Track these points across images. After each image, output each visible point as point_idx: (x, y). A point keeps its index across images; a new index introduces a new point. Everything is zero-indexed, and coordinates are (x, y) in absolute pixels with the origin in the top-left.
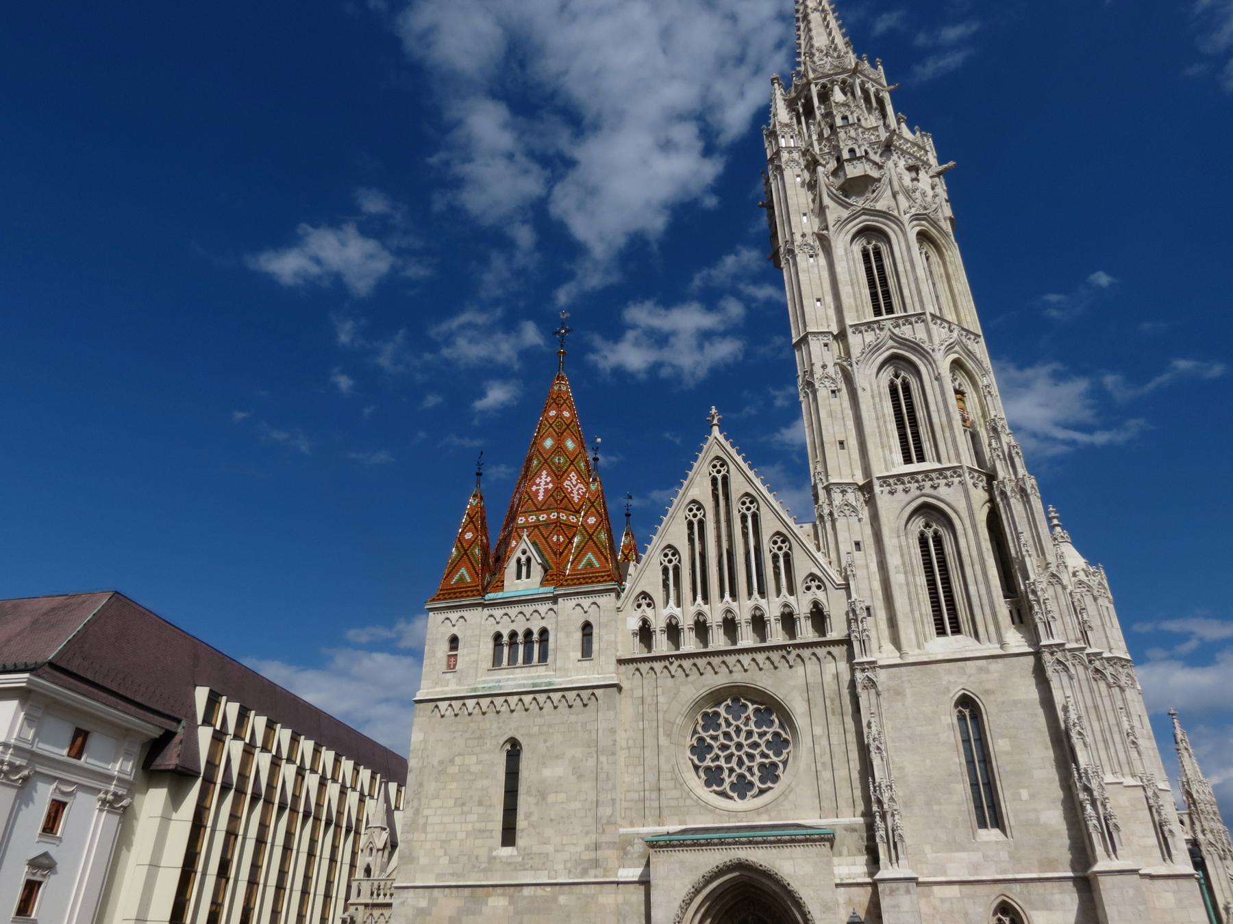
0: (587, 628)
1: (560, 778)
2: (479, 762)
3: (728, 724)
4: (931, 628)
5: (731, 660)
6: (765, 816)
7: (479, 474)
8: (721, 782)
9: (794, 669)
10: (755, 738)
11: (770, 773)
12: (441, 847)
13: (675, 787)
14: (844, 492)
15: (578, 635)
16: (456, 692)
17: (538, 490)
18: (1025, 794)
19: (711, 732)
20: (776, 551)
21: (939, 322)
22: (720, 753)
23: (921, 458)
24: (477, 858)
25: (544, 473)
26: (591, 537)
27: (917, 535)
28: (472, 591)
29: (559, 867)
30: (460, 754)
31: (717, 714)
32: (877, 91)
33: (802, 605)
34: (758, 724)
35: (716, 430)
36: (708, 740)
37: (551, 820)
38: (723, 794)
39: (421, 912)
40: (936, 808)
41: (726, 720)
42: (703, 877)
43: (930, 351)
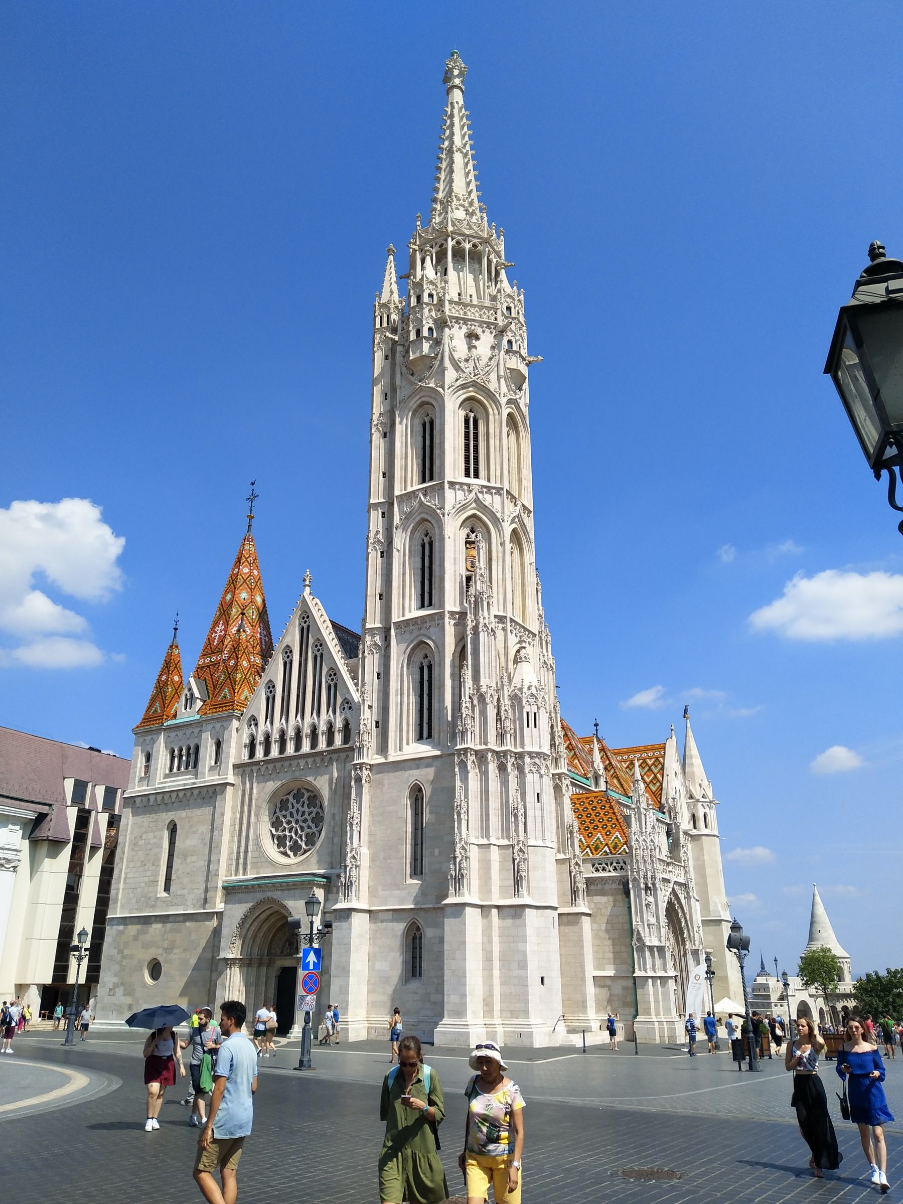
0: (218, 745)
1: (195, 846)
2: (155, 837)
3: (293, 808)
4: (412, 735)
5: (295, 762)
6: (301, 867)
7: (176, 629)
9: (328, 768)
12: (133, 892)
13: (257, 851)
14: (373, 636)
15: (214, 748)
16: (144, 791)
18: (437, 851)
20: (330, 682)
21: (457, 487)
22: (286, 826)
23: (430, 604)
24: (150, 898)
25: (222, 622)
26: (229, 677)
27: (418, 664)
28: (159, 720)
29: (189, 903)
30: (145, 832)
31: (288, 799)
32: (475, 246)
35: (308, 588)
37: (188, 874)
38: (285, 854)
39: (121, 933)
40: (389, 861)
42: (250, 909)
43: (441, 516)
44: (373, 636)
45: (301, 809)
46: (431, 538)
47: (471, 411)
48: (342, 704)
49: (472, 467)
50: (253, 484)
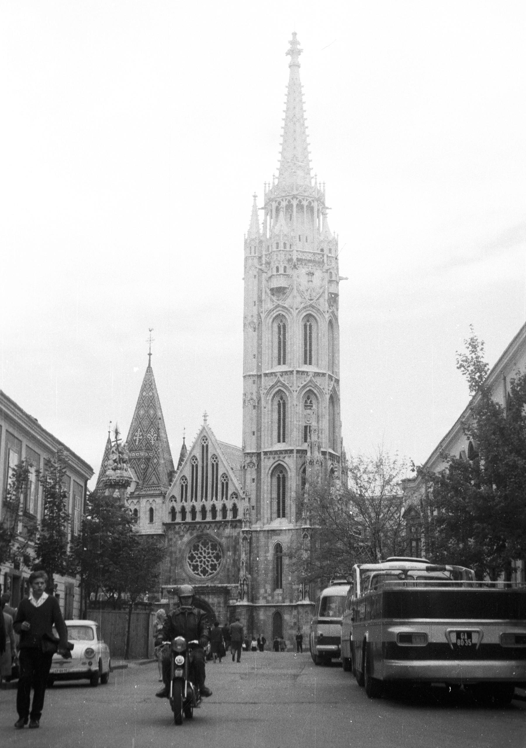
0: (151, 510)
3: (202, 549)
4: (275, 515)
5: (203, 525)
8: (198, 570)
10: (210, 555)
11: (214, 567)
14: (251, 457)
15: (148, 513)
17: (136, 439)
19: (196, 552)
20: (223, 481)
22: (198, 560)
31: (198, 546)
33: (229, 506)
34: (212, 550)
36: (195, 555)
38: (198, 574)
41: (201, 548)
44: (251, 457)
45: (207, 551)
46: (284, 401)
47: (308, 321)
48: (232, 495)
49: (308, 359)
50: (150, 331)
